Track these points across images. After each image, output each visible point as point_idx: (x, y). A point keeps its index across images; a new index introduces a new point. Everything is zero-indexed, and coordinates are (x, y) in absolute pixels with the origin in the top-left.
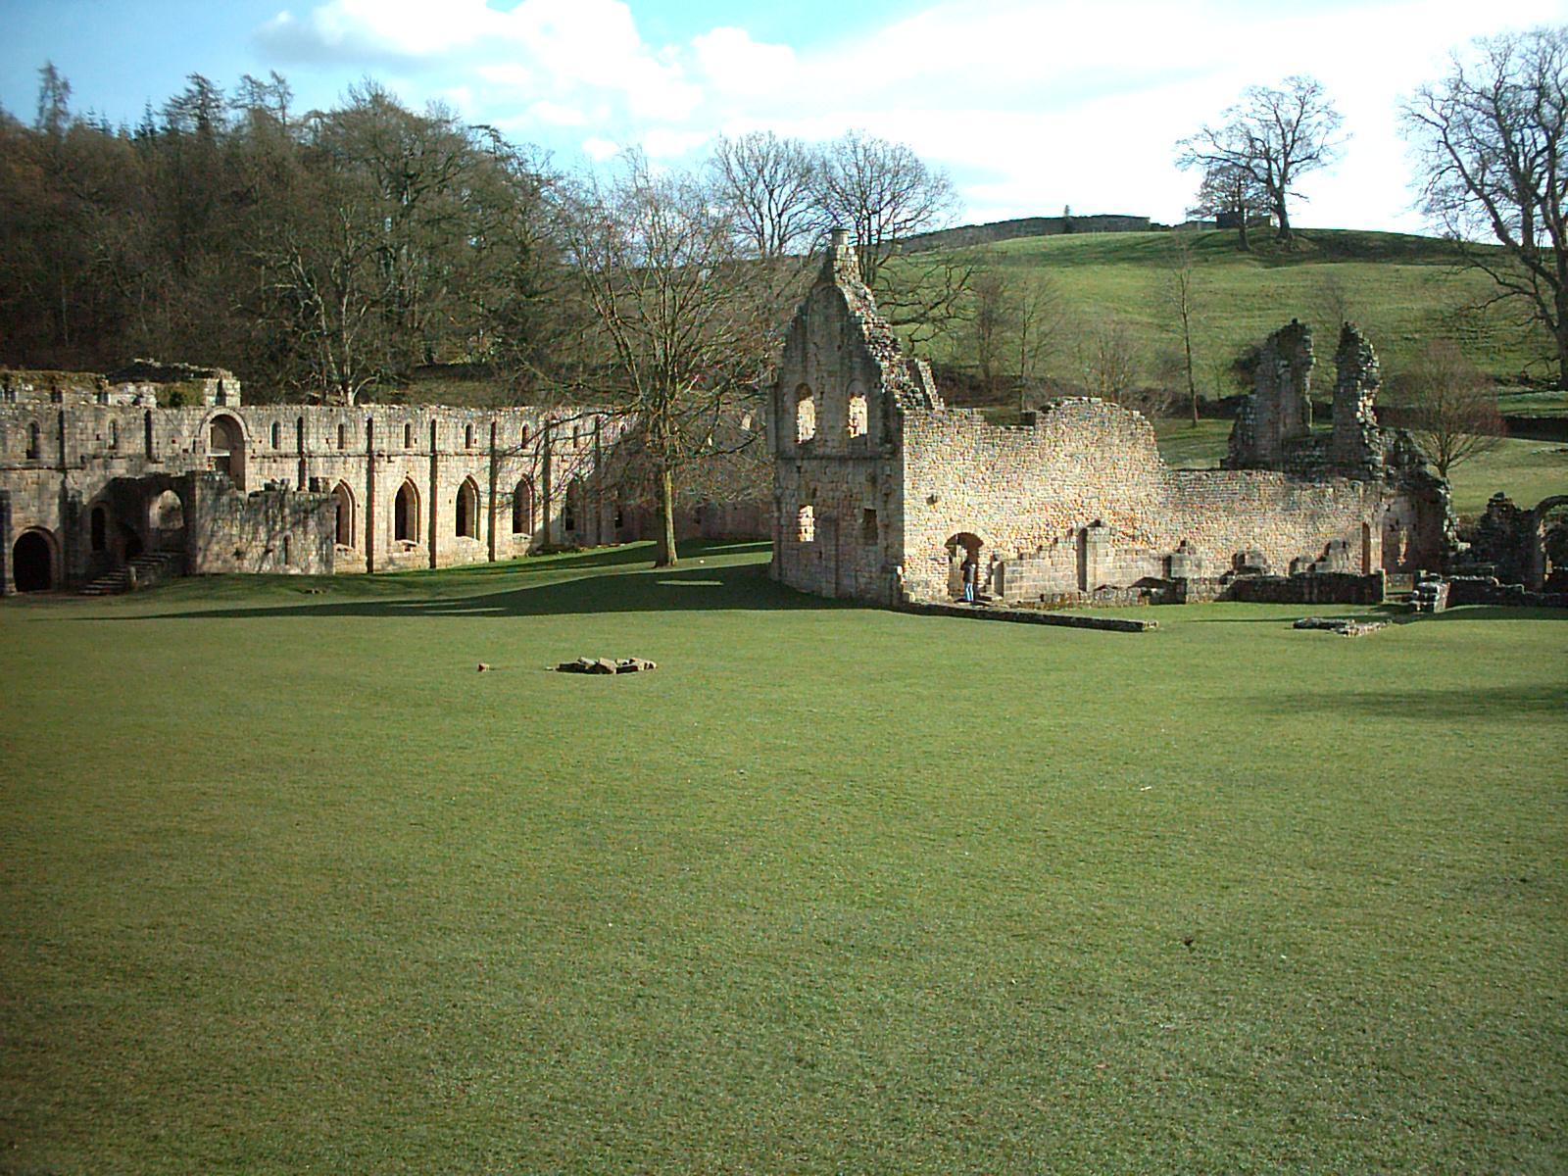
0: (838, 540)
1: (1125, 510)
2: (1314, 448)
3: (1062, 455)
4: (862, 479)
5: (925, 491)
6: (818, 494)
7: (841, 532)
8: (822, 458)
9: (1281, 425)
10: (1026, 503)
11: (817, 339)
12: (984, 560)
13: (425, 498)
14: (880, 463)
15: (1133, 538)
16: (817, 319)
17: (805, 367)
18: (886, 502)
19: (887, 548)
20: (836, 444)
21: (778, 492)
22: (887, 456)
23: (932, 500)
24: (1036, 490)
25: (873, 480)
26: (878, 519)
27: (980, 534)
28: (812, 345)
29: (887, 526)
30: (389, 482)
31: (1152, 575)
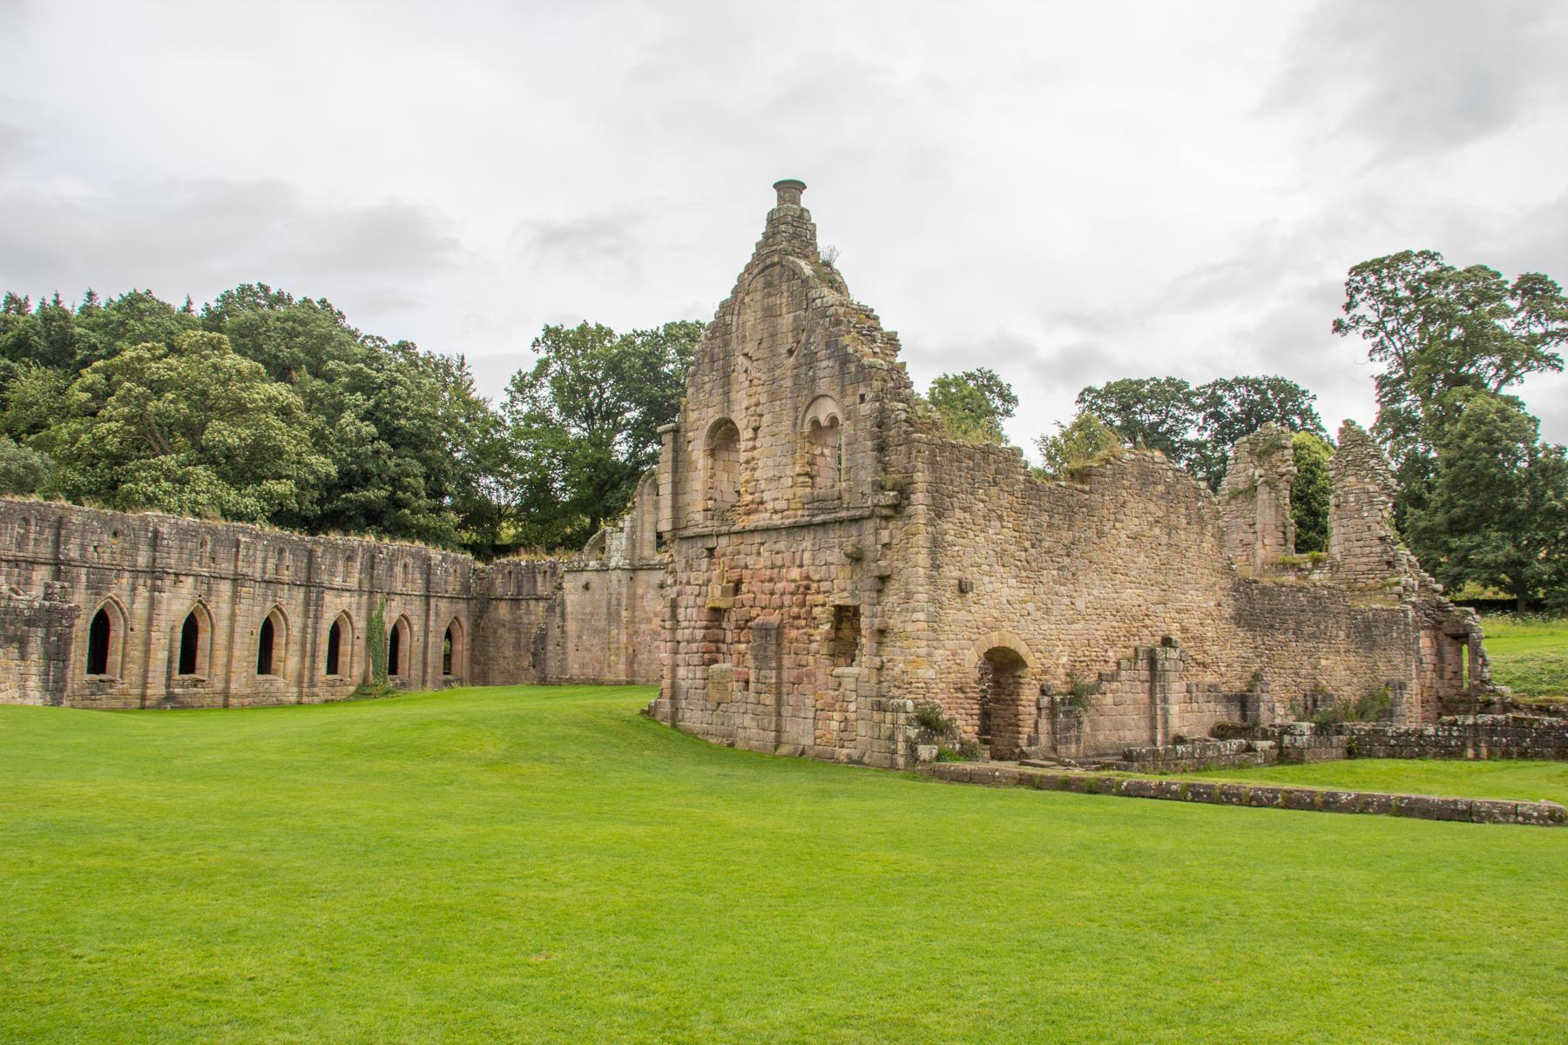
0: (779, 661)
1: (1196, 630)
2: (1310, 571)
3: (1123, 534)
4: (835, 556)
5: (952, 573)
6: (744, 588)
7: (786, 643)
8: (752, 531)
9: (1259, 545)
10: (1080, 604)
11: (750, 348)
12: (1029, 694)
13: (222, 625)
14: (869, 526)
15: (1204, 665)
16: (750, 317)
17: (727, 393)
18: (880, 591)
19: (880, 669)
20: (782, 505)
21: (672, 593)
22: (886, 512)
23: (963, 589)
24: (1093, 591)
25: (856, 558)
26: (864, 622)
27: (1023, 650)
28: (741, 359)
29: (882, 632)
30: (177, 604)
31: (1225, 720)
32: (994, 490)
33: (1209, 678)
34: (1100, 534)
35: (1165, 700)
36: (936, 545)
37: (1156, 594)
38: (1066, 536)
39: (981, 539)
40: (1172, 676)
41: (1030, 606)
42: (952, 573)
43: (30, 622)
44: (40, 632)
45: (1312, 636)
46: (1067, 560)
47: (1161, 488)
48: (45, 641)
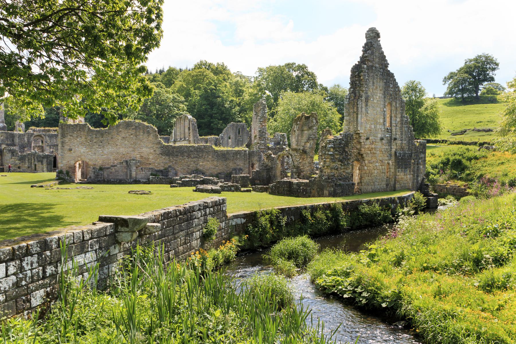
23: (70, 150)
32: (79, 132)
33: (151, 166)
34: (112, 138)
35: (131, 171)
36: (63, 143)
37: (131, 149)
38: (101, 139)
39: (76, 141)
40: (133, 166)
41: (90, 153)
42: (67, 147)
43: (43, 158)
44: (46, 160)
45: (194, 157)
46: (101, 144)
47: (133, 127)
48: (47, 161)
